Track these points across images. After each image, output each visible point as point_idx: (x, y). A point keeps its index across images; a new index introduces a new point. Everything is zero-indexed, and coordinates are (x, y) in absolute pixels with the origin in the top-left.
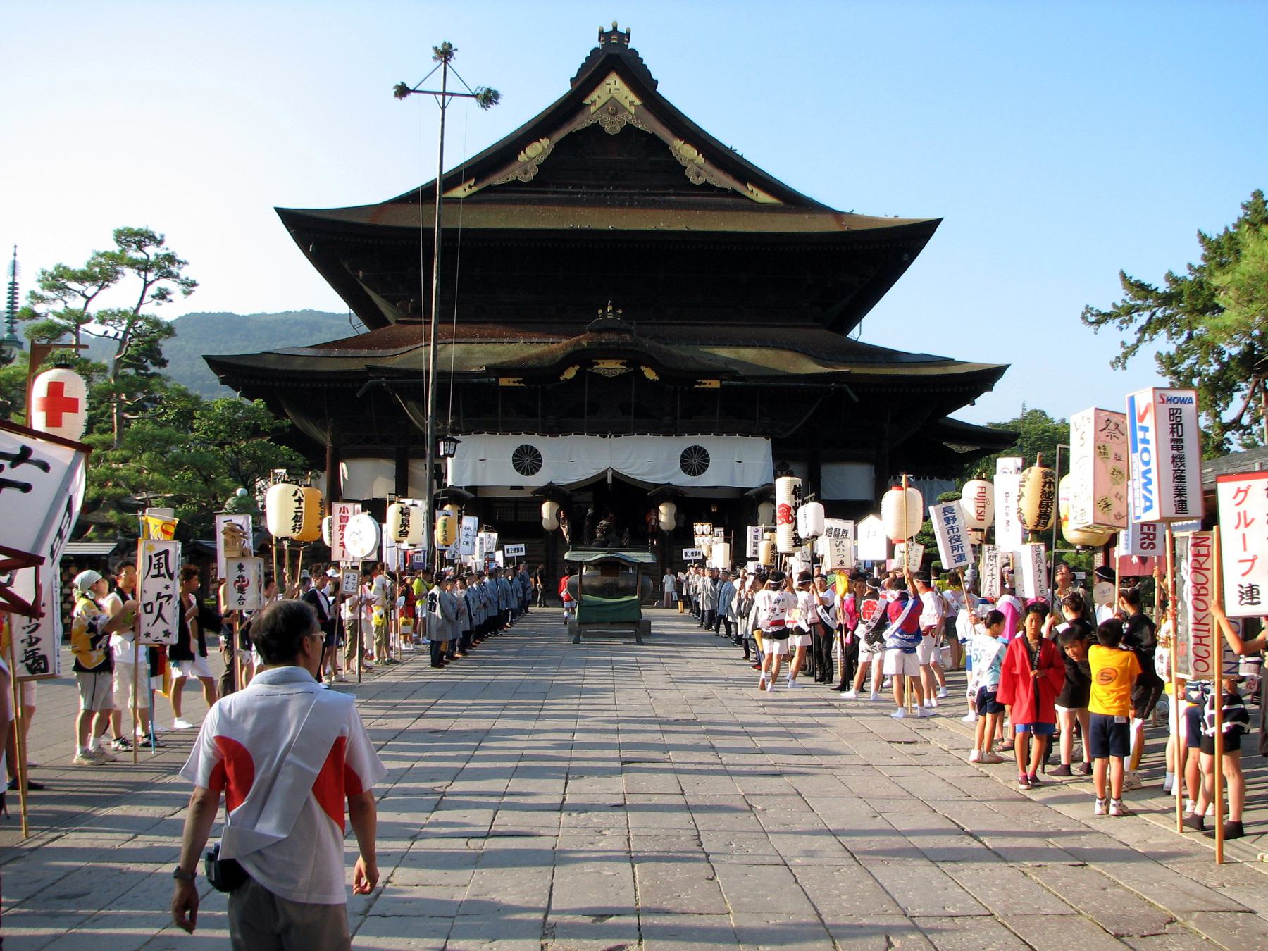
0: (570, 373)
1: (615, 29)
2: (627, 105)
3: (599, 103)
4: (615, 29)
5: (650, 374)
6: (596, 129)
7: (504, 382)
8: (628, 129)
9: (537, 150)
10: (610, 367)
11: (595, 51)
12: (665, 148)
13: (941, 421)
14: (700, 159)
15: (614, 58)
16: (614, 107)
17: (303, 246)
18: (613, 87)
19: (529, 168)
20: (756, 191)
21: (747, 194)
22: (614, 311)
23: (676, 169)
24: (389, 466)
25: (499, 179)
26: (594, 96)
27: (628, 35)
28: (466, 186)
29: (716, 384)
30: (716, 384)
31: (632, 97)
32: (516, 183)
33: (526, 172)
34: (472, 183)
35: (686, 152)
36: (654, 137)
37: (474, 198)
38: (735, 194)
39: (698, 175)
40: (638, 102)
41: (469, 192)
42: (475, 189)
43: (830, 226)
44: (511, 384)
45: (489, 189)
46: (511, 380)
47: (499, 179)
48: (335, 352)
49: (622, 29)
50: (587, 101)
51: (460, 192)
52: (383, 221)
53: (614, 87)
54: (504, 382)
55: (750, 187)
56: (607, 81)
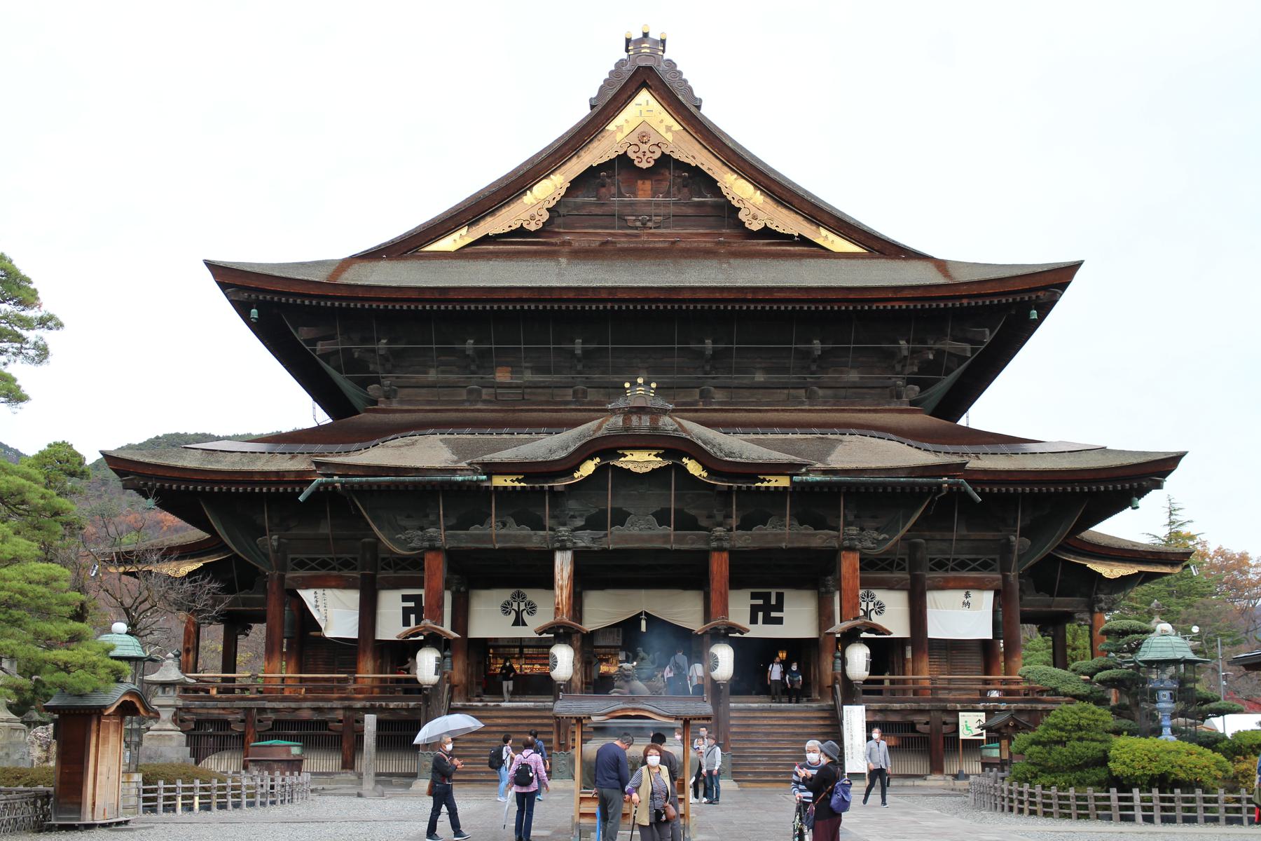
0: (588, 468)
1: (646, 35)
2: (662, 131)
3: (627, 131)
4: (646, 35)
5: (694, 468)
6: (623, 161)
7: (499, 481)
8: (665, 161)
9: (549, 189)
10: (640, 461)
11: (620, 64)
12: (711, 185)
13: (1085, 535)
14: (758, 198)
17: (242, 309)
20: (832, 236)
22: (647, 383)
23: (727, 212)
24: (352, 598)
27: (663, 42)
28: (456, 235)
29: (783, 482)
30: (783, 482)
31: (670, 121)
32: (521, 232)
33: (532, 218)
34: (464, 231)
35: (737, 188)
36: (697, 172)
37: (467, 250)
38: (804, 241)
39: (755, 218)
40: (677, 127)
42: (469, 240)
43: (932, 277)
44: (509, 484)
45: (486, 239)
46: (509, 478)
48: (281, 447)
50: (611, 127)
51: (449, 243)
52: (348, 278)
53: (645, 106)
54: (499, 481)
55: (823, 232)
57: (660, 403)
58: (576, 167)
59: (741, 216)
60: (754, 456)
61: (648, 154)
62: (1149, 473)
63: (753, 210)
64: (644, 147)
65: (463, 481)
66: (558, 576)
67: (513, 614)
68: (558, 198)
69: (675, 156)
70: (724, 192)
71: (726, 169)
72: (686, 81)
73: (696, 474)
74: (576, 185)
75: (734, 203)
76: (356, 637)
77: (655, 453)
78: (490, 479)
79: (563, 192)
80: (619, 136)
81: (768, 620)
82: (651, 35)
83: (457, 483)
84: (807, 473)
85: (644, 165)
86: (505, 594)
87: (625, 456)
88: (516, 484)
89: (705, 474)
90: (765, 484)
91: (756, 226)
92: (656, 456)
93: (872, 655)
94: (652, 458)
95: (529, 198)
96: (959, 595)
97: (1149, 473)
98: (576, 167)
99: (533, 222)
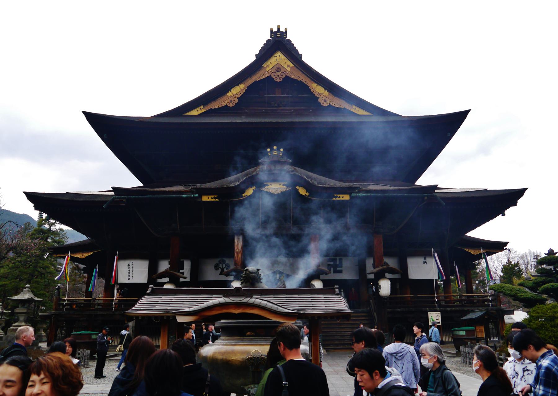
1: (279, 29)
2: (286, 67)
3: (271, 67)
4: (279, 29)
6: (269, 78)
7: (205, 198)
8: (287, 79)
9: (238, 90)
11: (268, 41)
12: (306, 89)
14: (326, 93)
15: (279, 43)
16: (278, 68)
18: (278, 57)
19: (232, 99)
20: (357, 109)
21: (353, 110)
22: (278, 149)
23: (314, 98)
25: (217, 105)
26: (268, 63)
27: (286, 32)
28: (198, 109)
29: (347, 197)
30: (347, 197)
31: (289, 63)
33: (231, 101)
34: (202, 107)
35: (318, 89)
39: (325, 101)
40: (292, 65)
41: (200, 112)
42: (203, 111)
44: (210, 200)
46: (210, 197)
47: (217, 105)
49: (282, 30)
50: (265, 65)
51: (195, 112)
53: (279, 58)
54: (205, 198)
55: (354, 107)
56: (276, 55)
57: (285, 159)
58: (250, 81)
59: (320, 100)
60: (332, 184)
61: (280, 76)
62: (507, 199)
63: (324, 98)
64: (278, 73)
65: (187, 197)
66: (236, 248)
67: (220, 270)
68: (242, 94)
69: (292, 77)
70: (312, 90)
71: (312, 82)
72: (295, 48)
73: (303, 194)
74: (249, 89)
75: (316, 95)
76: (146, 282)
77: (283, 183)
78: (200, 197)
79: (244, 91)
80: (268, 69)
81: (336, 272)
82: (281, 30)
83: (183, 198)
84: (359, 192)
85: (278, 80)
86: (216, 261)
87: (268, 185)
88: (214, 200)
89: (308, 194)
90: (338, 199)
91: (325, 104)
92: (283, 185)
93: (391, 285)
94: (281, 186)
95: (229, 94)
96: (421, 260)
97: (507, 199)
98: (250, 81)
99: (231, 103)
